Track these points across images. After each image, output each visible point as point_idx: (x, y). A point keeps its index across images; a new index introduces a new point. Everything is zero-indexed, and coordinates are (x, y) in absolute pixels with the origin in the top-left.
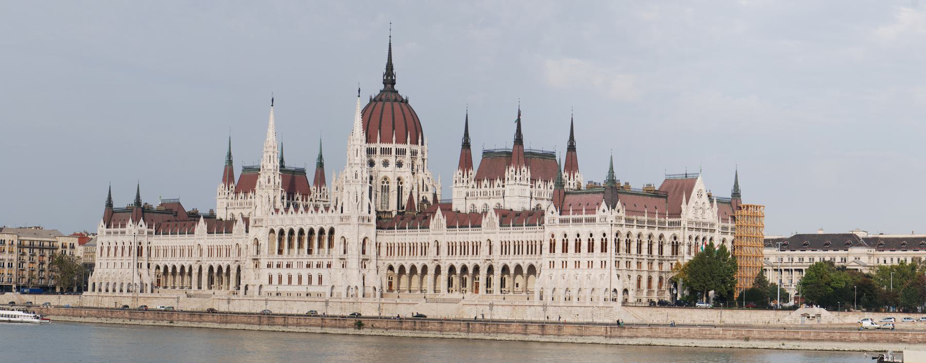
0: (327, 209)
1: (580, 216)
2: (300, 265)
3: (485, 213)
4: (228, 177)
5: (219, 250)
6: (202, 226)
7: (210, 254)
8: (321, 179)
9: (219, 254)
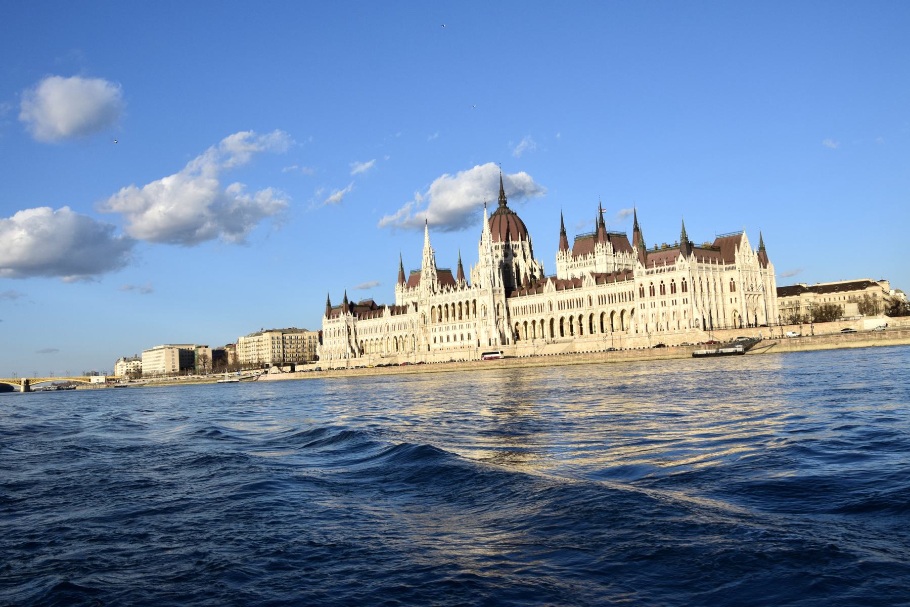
0: (469, 287)
1: (662, 268)
2: (454, 328)
3: (583, 277)
4: (402, 278)
5: (399, 326)
6: (387, 312)
7: (394, 329)
8: (462, 275)
9: (400, 328)
